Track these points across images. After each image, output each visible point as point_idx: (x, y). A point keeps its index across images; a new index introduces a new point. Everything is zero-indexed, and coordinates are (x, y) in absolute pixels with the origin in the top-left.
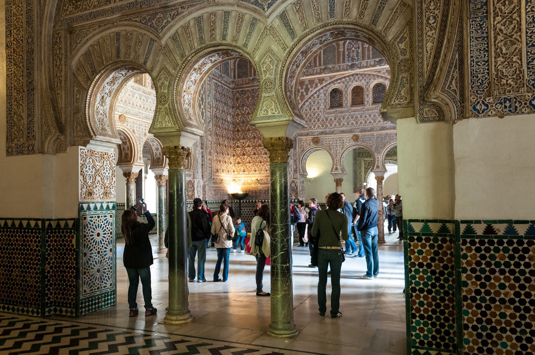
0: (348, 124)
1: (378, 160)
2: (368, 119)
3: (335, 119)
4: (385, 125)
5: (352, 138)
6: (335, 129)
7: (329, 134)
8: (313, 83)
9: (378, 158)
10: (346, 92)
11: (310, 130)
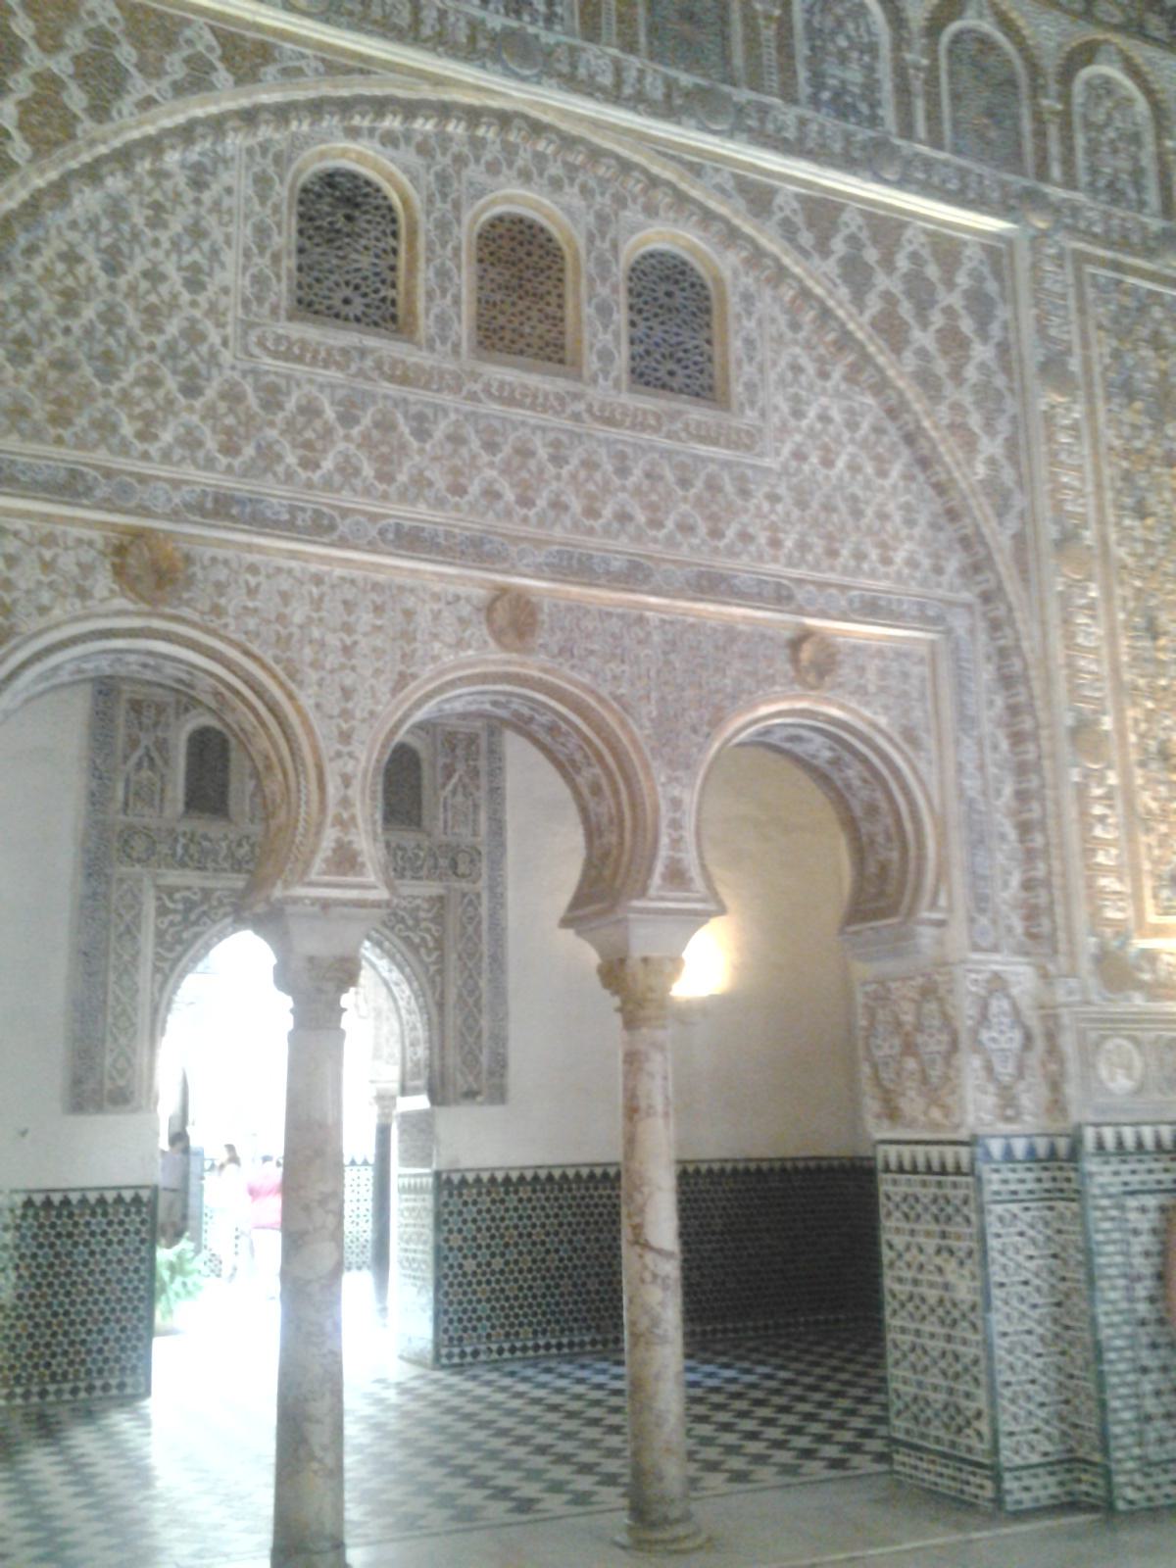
0: (459, 490)
1: (676, 825)
2: (606, 488)
3: (348, 419)
4: (723, 564)
5: (490, 609)
6: (347, 499)
7: (288, 526)
8: (170, 42)
9: (676, 803)
10: (443, 226)
11: (101, 456)
